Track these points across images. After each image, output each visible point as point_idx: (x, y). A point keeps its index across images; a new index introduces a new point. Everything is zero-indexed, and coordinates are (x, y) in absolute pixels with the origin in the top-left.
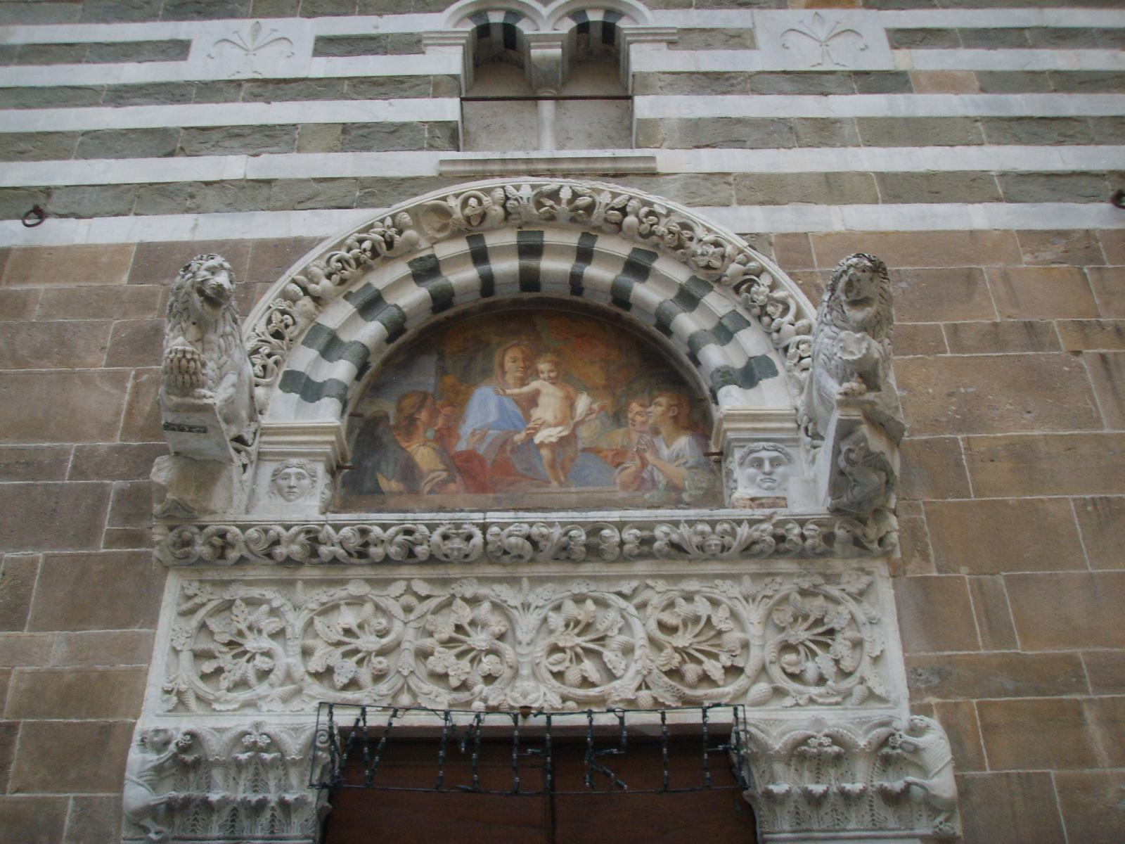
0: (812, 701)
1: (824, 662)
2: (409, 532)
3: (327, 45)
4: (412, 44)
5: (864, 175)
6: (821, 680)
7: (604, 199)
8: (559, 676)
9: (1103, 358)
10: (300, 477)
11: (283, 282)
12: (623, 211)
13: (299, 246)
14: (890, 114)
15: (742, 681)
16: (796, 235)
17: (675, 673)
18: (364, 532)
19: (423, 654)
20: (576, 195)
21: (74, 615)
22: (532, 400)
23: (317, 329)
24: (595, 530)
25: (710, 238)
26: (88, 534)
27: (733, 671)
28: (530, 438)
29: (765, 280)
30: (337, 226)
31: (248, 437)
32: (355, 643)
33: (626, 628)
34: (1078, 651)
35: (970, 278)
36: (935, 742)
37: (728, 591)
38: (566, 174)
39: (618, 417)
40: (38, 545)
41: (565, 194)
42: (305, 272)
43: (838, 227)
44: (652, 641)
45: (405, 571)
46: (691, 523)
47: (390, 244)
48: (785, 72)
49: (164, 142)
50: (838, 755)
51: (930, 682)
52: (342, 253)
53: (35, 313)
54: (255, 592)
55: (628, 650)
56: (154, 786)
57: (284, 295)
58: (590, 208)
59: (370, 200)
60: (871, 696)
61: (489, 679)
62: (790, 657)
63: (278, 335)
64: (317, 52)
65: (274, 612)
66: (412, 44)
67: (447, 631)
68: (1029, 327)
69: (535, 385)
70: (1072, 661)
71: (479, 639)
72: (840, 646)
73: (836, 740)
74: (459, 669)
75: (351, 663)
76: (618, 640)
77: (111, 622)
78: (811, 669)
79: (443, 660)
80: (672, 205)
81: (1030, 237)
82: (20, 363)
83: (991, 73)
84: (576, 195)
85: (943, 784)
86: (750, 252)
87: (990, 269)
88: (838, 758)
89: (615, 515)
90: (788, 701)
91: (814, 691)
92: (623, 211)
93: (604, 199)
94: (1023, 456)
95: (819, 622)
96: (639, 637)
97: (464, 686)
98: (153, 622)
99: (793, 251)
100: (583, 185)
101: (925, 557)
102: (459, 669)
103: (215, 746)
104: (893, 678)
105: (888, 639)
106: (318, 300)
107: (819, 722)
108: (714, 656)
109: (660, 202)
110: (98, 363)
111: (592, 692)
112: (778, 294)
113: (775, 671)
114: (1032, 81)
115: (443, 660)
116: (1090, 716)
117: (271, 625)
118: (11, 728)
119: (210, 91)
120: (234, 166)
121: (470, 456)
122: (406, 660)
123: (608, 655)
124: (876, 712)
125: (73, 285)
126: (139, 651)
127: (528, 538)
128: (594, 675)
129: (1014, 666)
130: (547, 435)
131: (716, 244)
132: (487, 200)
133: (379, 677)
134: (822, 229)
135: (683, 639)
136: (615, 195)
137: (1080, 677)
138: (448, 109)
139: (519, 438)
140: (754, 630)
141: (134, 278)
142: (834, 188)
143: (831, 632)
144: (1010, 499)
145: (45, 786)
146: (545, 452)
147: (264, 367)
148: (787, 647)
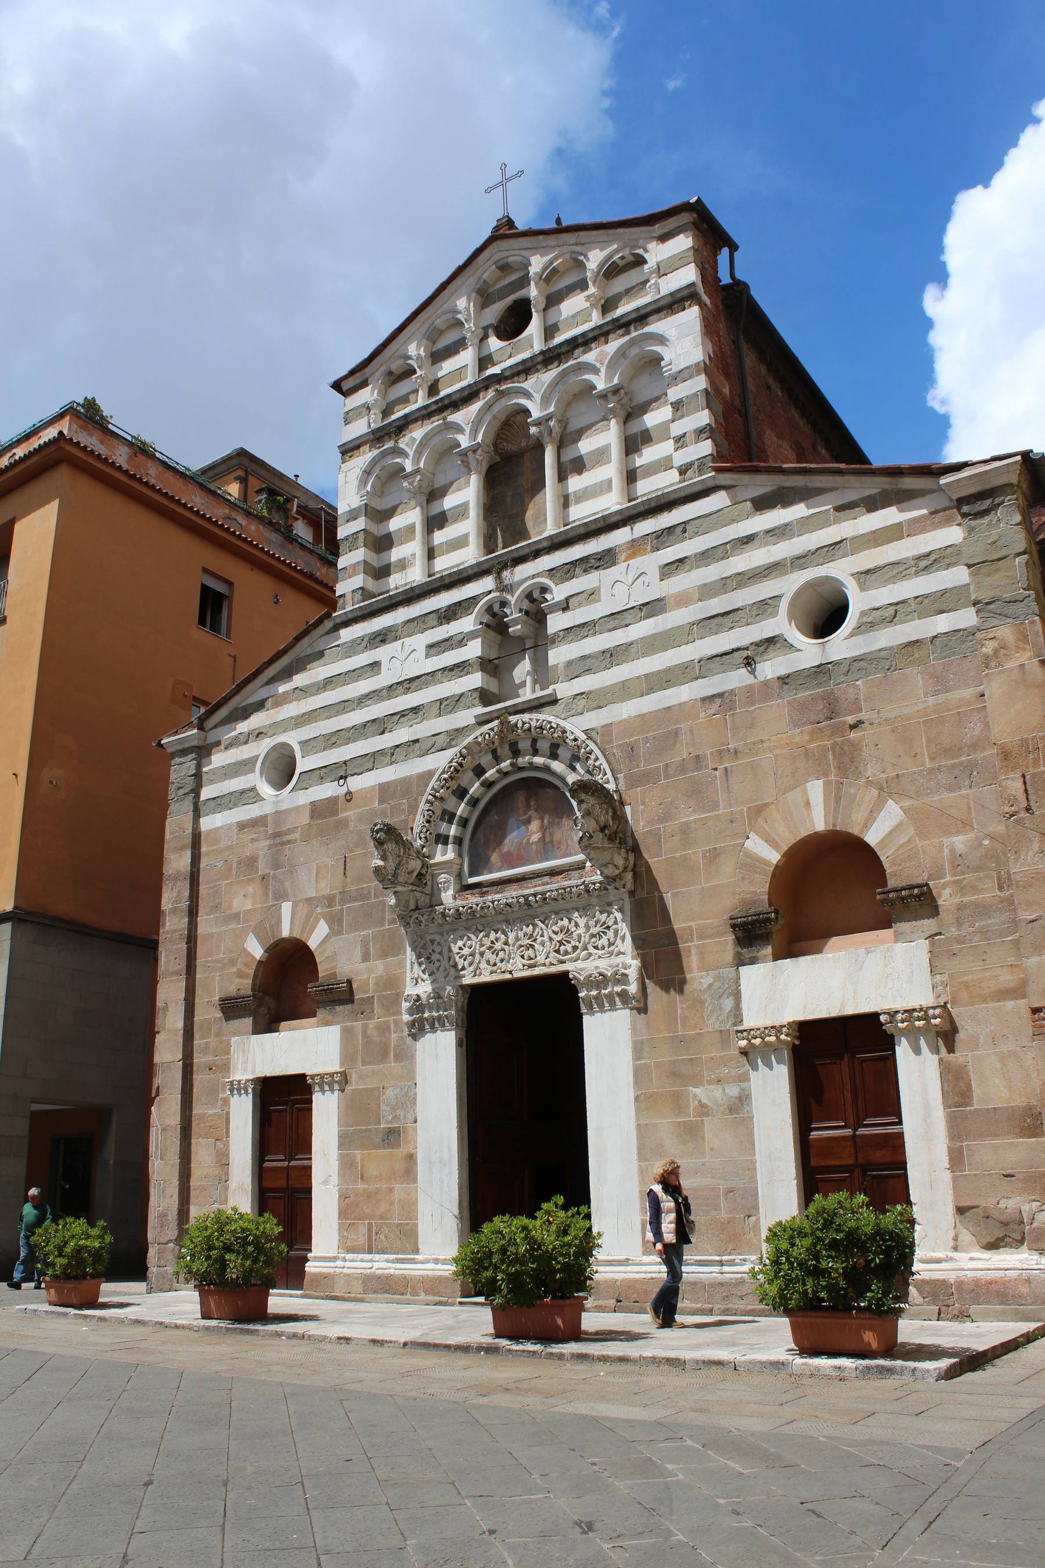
0: (600, 957)
1: (604, 941)
2: (471, 908)
5: (639, 677)
6: (603, 948)
7: (533, 724)
8: (522, 957)
9: (726, 769)
10: (445, 882)
11: (426, 794)
12: (541, 728)
13: (430, 774)
14: (655, 631)
15: (578, 951)
16: (607, 725)
17: (557, 951)
18: (458, 910)
19: (482, 954)
20: (524, 723)
21: (384, 954)
23: (444, 812)
24: (526, 897)
25: (572, 737)
26: (382, 921)
27: (575, 948)
28: (529, 840)
29: (593, 757)
30: (439, 761)
31: (424, 871)
32: (463, 952)
33: (542, 936)
34: (693, 924)
35: (676, 733)
38: (522, 712)
40: (369, 928)
41: (520, 725)
42: (433, 789)
43: (625, 716)
44: (551, 939)
45: (474, 922)
46: (557, 890)
47: (461, 765)
48: (613, 614)
50: (603, 980)
52: (446, 776)
53: (352, 825)
54: (432, 937)
55: (543, 944)
56: (412, 1015)
57: (428, 802)
58: (529, 730)
59: (453, 743)
60: (620, 953)
61: (502, 961)
62: (594, 940)
63: (428, 821)
64: (427, 656)
65: (439, 944)
67: (489, 944)
68: (698, 757)
69: (530, 813)
70: (690, 929)
71: (498, 945)
72: (611, 933)
73: (601, 974)
74: (493, 958)
75: (462, 960)
76: (540, 939)
77: (394, 955)
78: (600, 943)
80: (559, 721)
82: (352, 851)
83: (705, 584)
84: (524, 723)
86: (587, 742)
87: (684, 726)
88: (603, 982)
89: (532, 891)
90: (592, 958)
91: (601, 952)
92: (541, 728)
93: (533, 724)
94: (685, 830)
95: (604, 923)
96: (546, 938)
97: (495, 965)
98: (405, 953)
100: (526, 717)
101: (643, 889)
102: (493, 958)
106: (442, 799)
107: (597, 968)
108: (569, 942)
111: (532, 962)
112: (597, 764)
113: (590, 947)
114: (725, 584)
115: (488, 955)
116: (693, 952)
117: (438, 949)
118: (373, 997)
119: (391, 691)
121: (509, 853)
122: (477, 956)
123: (537, 946)
124: (620, 959)
125: (360, 810)
126: (402, 964)
127: (507, 904)
128: (533, 956)
131: (575, 740)
132: (492, 734)
133: (470, 964)
134: (617, 719)
135: (559, 937)
136: (538, 720)
137: (692, 935)
138: (476, 680)
139: (524, 841)
140: (581, 930)
141: (381, 802)
142: (625, 691)
143: (608, 928)
144: (677, 855)
145: (385, 1016)
146: (534, 847)
147: (426, 838)
148: (593, 936)
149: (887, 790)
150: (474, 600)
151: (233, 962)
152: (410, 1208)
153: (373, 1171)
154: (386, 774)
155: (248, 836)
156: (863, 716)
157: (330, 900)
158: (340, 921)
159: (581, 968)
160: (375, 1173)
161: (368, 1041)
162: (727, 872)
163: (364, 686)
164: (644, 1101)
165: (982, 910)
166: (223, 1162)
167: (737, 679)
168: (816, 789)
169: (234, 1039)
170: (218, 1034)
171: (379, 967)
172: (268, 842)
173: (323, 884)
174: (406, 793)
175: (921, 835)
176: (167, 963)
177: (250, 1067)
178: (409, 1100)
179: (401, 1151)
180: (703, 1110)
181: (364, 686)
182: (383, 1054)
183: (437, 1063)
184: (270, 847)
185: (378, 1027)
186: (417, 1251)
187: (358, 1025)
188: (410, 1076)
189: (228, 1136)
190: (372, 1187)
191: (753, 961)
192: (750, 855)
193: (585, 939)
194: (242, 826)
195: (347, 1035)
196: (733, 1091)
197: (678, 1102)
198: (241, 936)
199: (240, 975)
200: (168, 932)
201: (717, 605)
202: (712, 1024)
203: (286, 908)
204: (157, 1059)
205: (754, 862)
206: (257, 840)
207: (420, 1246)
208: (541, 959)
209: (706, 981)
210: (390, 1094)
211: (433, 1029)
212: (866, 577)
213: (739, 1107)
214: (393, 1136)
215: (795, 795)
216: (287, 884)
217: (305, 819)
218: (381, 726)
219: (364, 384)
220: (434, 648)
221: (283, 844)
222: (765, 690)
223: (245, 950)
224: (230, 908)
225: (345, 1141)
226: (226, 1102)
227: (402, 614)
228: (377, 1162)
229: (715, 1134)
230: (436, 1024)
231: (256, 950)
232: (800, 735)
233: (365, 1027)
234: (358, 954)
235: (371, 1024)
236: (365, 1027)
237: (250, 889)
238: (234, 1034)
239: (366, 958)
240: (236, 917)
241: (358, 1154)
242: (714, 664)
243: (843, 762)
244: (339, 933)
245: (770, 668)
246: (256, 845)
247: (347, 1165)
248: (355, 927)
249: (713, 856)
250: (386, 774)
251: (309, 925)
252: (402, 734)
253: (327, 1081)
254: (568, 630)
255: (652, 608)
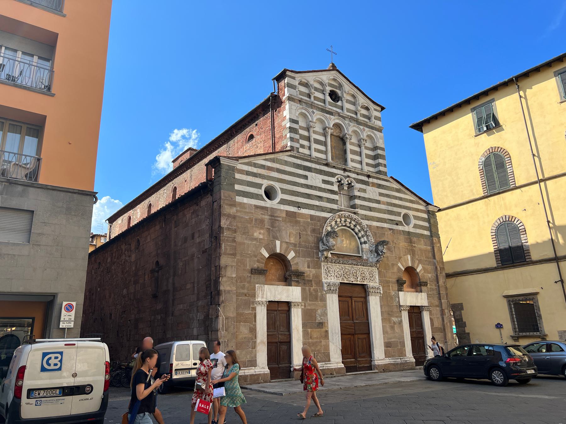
3: (324, 182)
4: (331, 184)
13: (326, 219)
22: (343, 241)
35: (384, 234)
36: (381, 288)
37: (366, 270)
39: (350, 244)
49: (309, 196)
51: (381, 282)
53: (301, 224)
66: (331, 184)
79: (345, 275)
81: (390, 229)
85: (382, 292)
87: (386, 233)
94: (387, 257)
99: (369, 227)
100: (352, 215)
103: (331, 284)
104: (377, 280)
105: (377, 277)
109: (359, 219)
110: (309, 232)
115: (345, 275)
120: (317, 203)
129: (386, 280)
130: (345, 245)
149: (420, 262)
150: (337, 174)
151: (255, 256)
152: (327, 347)
153: (315, 335)
154: (312, 212)
155: (259, 212)
156: (416, 245)
157: (295, 245)
158: (299, 253)
159: (371, 284)
160: (315, 336)
161: (311, 294)
162: (395, 270)
163: (302, 181)
164: (383, 320)
165: (433, 290)
166: (253, 330)
167: (395, 227)
168: (409, 257)
169: (257, 285)
170: (249, 282)
171: (314, 271)
172: (268, 217)
173: (292, 239)
174: (319, 221)
175: (425, 272)
176: (226, 249)
177: (265, 296)
178: (325, 314)
179: (324, 330)
180: (394, 323)
181: (302, 181)
182: (316, 298)
183: (333, 303)
184: (270, 219)
185: (314, 290)
186: (329, 361)
187: (307, 288)
188: (325, 306)
189: (255, 321)
190: (315, 340)
191: (401, 291)
192: (399, 267)
193: (368, 277)
194: (257, 207)
195: (303, 291)
196: (399, 319)
197: (390, 321)
198: (258, 248)
199: (258, 261)
200: (225, 237)
201: (390, 208)
202: (395, 304)
203: (278, 243)
204: (222, 288)
205: (399, 269)
206: (264, 215)
207: (331, 359)
208: (359, 279)
209: (393, 293)
210: (319, 311)
211: (332, 293)
212: (416, 218)
213: (401, 322)
214: (321, 325)
215: (406, 257)
216: (278, 234)
217: (284, 215)
218: (309, 196)
219: (294, 78)
220: (324, 182)
221: (275, 220)
222: (400, 232)
223: (261, 253)
224: (253, 235)
225: (304, 325)
226: (254, 309)
227: (313, 166)
228: (316, 333)
229: (397, 329)
230: (332, 292)
231: (267, 255)
232: (406, 244)
233: (310, 289)
234: (306, 265)
235: (312, 289)
236: (310, 289)
237: (262, 231)
238: (257, 284)
239: (309, 267)
240: (256, 239)
241: (309, 330)
242: (390, 222)
243: (412, 252)
244: (299, 257)
245: (400, 228)
246: (263, 216)
247: (305, 333)
248: (304, 256)
249: (393, 265)
250: (312, 212)
251: (288, 250)
252: (317, 203)
253: (297, 304)
254: (359, 197)
255: (378, 202)
